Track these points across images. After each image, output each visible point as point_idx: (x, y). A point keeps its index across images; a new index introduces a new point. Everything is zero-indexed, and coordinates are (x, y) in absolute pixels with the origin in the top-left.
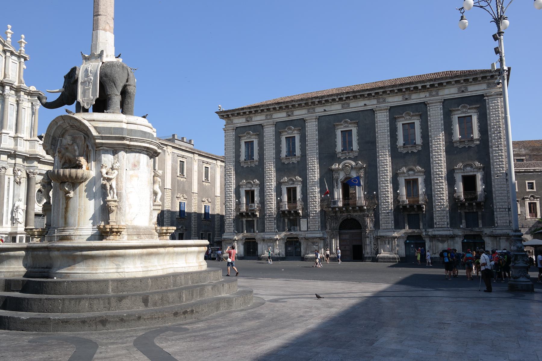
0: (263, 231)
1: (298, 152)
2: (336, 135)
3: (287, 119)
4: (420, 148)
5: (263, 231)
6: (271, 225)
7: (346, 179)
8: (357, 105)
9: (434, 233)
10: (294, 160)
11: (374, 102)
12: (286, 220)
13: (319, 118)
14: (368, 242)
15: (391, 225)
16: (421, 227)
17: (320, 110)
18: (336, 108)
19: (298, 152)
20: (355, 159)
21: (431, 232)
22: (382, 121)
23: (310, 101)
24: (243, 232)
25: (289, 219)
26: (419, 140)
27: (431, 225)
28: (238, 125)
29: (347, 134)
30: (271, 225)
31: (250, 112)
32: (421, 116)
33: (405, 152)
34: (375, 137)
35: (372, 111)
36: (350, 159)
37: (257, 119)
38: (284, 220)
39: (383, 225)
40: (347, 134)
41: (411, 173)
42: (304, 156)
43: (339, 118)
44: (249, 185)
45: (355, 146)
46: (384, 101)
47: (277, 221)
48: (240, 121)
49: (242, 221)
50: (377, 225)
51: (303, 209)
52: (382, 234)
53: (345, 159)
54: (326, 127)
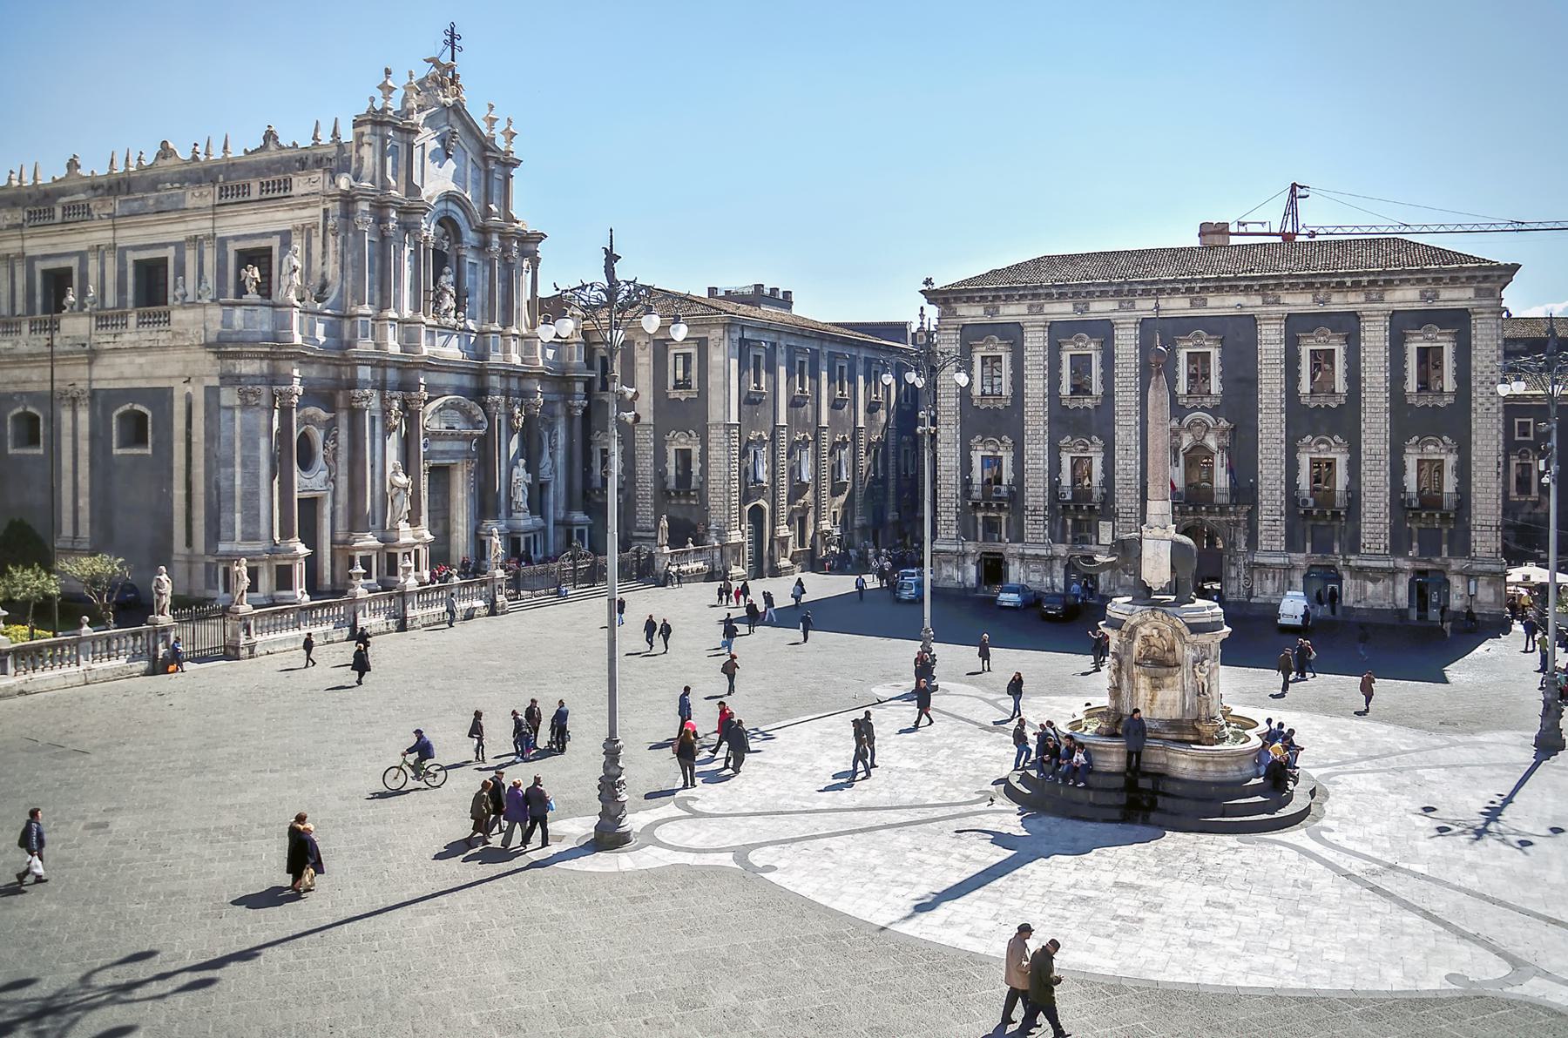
0: (1019, 538)
1: (1097, 388)
2: (1177, 359)
3: (1075, 317)
4: (1343, 401)
5: (1019, 538)
6: (1036, 527)
7: (1194, 448)
8: (1222, 304)
9: (1359, 563)
10: (1089, 402)
11: (1258, 300)
12: (1069, 522)
13: (1144, 323)
14: (1233, 574)
15: (1279, 545)
16: (1336, 550)
17: (1145, 307)
18: (1177, 306)
19: (1097, 388)
20: (1214, 411)
21: (1355, 561)
22: (1270, 340)
23: (1126, 287)
24: (976, 539)
25: (1075, 521)
26: (1340, 386)
27: (1354, 546)
28: (968, 321)
29: (1199, 360)
30: (1036, 527)
31: (996, 298)
32: (1347, 339)
33: (1312, 405)
34: (1256, 372)
35: (1253, 320)
36: (1204, 409)
37: (1011, 312)
38: (1064, 522)
39: (1264, 542)
40: (1199, 360)
41: (1322, 446)
42: (1109, 395)
43: (1184, 326)
44: (992, 447)
45: (1215, 386)
46: (1277, 302)
47: (1050, 521)
48: (972, 313)
49: (976, 518)
50: (1252, 542)
51: (1103, 503)
52: (1261, 560)
53: (1195, 409)
54: (1160, 337)
